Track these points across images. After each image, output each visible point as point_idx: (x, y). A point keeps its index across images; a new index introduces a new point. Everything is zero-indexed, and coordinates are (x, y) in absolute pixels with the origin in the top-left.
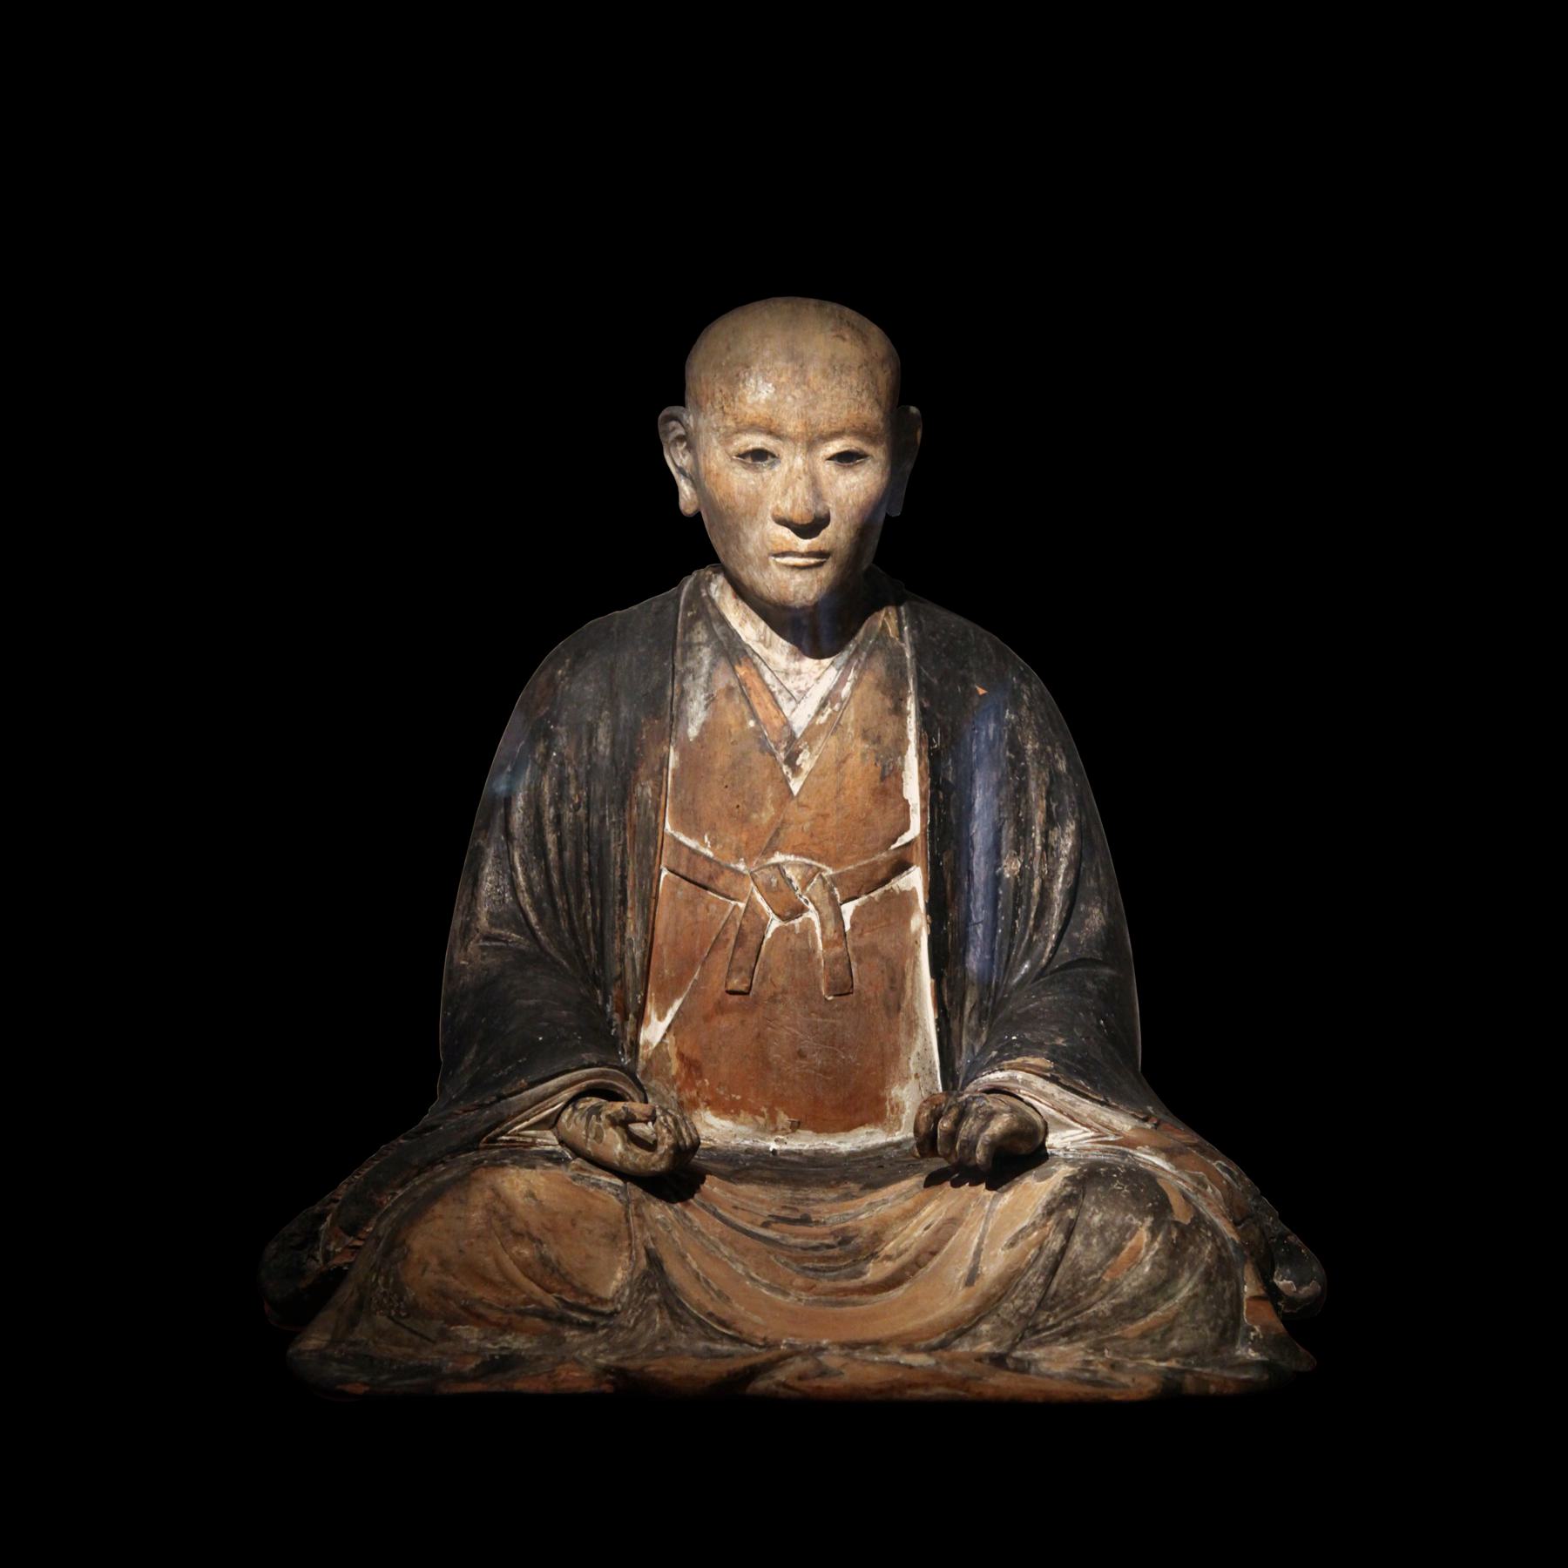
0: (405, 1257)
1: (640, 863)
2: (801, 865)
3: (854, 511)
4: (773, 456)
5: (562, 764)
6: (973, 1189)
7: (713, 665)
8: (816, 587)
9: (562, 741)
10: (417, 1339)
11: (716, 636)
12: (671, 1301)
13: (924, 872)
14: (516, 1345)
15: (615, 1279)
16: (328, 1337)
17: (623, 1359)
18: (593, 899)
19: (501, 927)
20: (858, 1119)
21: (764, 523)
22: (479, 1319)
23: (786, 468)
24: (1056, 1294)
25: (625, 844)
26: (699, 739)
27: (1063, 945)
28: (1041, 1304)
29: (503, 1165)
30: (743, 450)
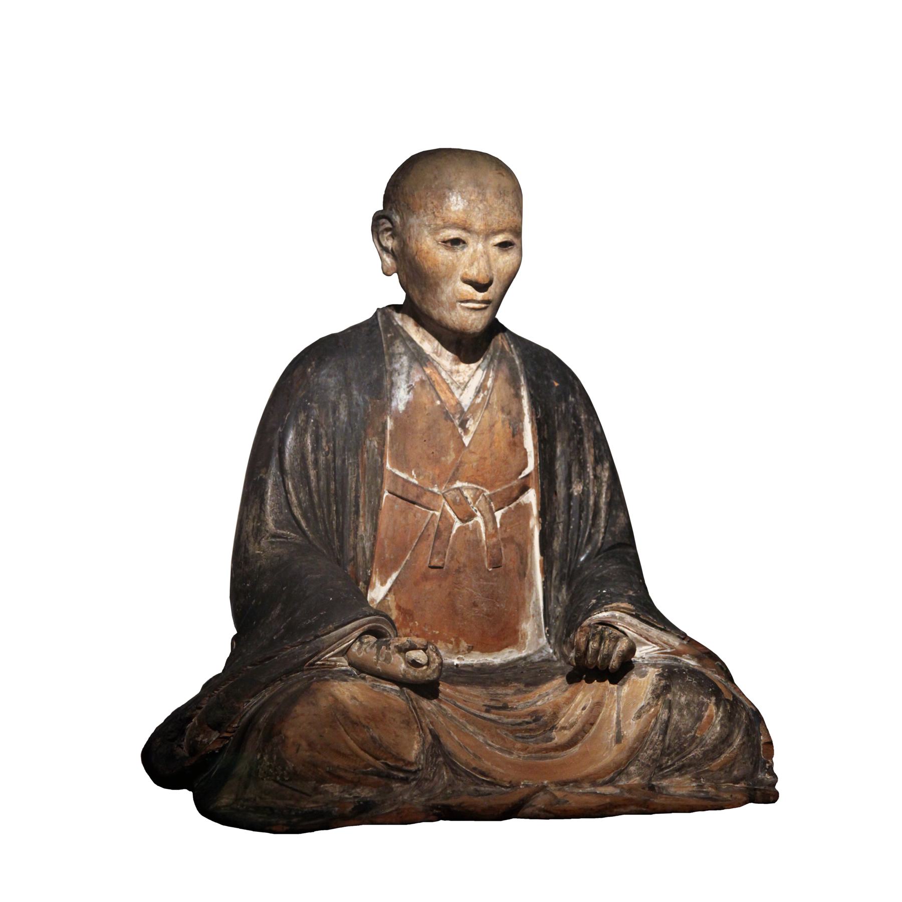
0: (283, 741)
1: (370, 488)
2: (472, 489)
3: (506, 277)
4: (464, 242)
5: (317, 427)
6: (603, 684)
7: (410, 367)
8: (483, 321)
9: (316, 412)
10: (297, 795)
11: (410, 350)
12: (450, 762)
13: (537, 492)
14: (363, 795)
15: (414, 749)
16: (233, 796)
17: (429, 800)
18: (337, 511)
19: (282, 529)
20: (505, 643)
21: (455, 282)
22: (339, 779)
23: (471, 250)
24: (669, 746)
25: (358, 476)
26: (405, 412)
27: (608, 535)
28: (663, 754)
29: (327, 680)
30: (447, 238)
